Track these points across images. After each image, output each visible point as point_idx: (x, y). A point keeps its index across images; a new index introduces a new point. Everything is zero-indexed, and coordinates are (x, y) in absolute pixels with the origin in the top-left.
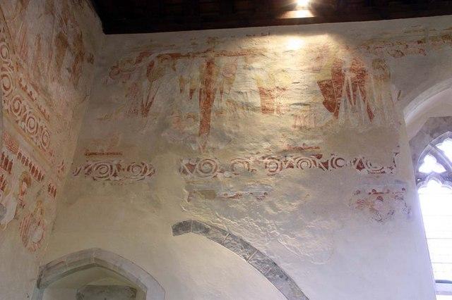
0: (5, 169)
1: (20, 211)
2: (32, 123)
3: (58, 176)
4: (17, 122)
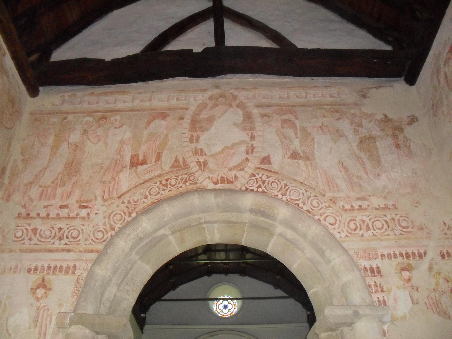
0: (375, 276)
1: (416, 295)
2: (379, 224)
4: (362, 236)
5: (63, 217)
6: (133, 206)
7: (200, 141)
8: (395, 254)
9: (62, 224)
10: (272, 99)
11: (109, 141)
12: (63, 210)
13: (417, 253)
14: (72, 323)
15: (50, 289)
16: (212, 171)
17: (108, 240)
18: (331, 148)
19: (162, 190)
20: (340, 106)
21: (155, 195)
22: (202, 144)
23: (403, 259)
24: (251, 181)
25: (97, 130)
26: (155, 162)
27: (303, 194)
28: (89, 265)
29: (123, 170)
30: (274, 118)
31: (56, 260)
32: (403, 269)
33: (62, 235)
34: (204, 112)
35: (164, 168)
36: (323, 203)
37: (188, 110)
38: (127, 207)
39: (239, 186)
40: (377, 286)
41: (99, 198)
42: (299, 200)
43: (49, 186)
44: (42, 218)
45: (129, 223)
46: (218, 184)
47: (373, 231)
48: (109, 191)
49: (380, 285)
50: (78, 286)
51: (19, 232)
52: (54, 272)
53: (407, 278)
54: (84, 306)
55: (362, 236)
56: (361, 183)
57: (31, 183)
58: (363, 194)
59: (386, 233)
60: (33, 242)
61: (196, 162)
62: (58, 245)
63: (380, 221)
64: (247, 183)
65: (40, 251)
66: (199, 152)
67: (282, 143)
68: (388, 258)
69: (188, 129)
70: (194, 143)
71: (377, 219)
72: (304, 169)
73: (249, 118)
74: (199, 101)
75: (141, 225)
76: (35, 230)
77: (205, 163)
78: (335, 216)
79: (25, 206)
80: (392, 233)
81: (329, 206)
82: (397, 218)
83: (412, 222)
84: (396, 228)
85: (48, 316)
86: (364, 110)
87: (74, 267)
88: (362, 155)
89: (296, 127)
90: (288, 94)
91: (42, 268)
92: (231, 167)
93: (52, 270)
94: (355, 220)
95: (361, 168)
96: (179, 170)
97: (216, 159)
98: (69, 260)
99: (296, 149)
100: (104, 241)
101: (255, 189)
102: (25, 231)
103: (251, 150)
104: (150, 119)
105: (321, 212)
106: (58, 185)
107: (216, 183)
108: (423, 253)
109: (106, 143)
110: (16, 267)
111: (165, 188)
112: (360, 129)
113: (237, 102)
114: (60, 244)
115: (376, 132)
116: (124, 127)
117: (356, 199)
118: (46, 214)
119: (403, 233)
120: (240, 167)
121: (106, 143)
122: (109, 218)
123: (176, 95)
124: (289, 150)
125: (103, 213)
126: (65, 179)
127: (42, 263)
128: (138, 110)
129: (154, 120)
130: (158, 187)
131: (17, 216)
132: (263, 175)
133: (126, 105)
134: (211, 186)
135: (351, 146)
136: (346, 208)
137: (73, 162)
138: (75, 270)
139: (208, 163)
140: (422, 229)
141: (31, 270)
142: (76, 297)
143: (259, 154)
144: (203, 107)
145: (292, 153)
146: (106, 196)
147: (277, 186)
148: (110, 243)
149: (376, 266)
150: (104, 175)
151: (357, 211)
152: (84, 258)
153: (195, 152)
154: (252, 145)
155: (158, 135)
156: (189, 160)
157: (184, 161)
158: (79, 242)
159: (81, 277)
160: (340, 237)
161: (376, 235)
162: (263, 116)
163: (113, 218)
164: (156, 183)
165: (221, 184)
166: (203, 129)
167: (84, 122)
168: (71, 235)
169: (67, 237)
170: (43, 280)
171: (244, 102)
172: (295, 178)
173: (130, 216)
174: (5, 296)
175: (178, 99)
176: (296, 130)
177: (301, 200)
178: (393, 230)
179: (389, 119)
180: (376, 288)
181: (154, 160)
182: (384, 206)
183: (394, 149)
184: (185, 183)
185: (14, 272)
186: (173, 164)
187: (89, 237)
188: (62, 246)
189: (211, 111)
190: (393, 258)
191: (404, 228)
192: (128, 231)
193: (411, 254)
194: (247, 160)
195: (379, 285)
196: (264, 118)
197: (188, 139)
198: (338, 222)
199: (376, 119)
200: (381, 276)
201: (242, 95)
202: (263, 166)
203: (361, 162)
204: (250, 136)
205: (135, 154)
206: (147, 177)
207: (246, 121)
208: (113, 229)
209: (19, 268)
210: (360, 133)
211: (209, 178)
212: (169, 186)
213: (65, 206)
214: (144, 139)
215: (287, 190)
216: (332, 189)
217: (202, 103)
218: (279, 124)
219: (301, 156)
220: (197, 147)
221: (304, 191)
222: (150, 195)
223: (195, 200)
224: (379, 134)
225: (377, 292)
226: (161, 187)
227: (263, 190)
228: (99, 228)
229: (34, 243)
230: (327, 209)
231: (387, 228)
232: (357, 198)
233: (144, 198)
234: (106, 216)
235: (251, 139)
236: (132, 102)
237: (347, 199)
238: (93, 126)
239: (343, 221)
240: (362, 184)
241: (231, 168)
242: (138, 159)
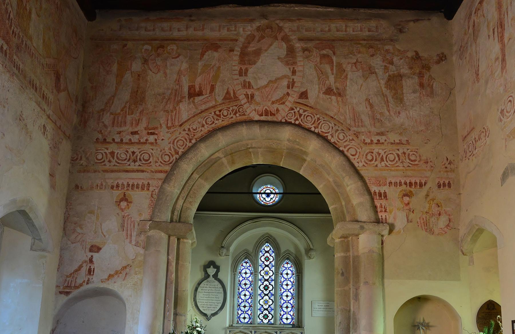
0: (381, 199)
1: (411, 216)
2: (391, 157)
3: (447, 172)
4: (377, 166)
5: (135, 142)
6: (192, 133)
8: (400, 182)
9: (135, 148)
11: (168, 71)
12: (134, 136)
13: (418, 183)
14: (151, 228)
15: (131, 202)
16: (258, 104)
17: (173, 162)
18: (362, 85)
19: (216, 120)
20: (376, 41)
21: (211, 124)
22: (249, 78)
23: (407, 187)
24: (290, 114)
25: (156, 59)
26: (210, 93)
27: (332, 128)
28: (160, 183)
29: (183, 100)
31: (133, 179)
32: (405, 195)
33: (135, 158)
34: (251, 45)
35: (217, 100)
36: (348, 136)
37: (238, 42)
38: (188, 134)
39: (280, 119)
40: (382, 207)
41: (164, 126)
42: (329, 132)
43: (119, 114)
44: (117, 143)
45: (190, 149)
46: (263, 116)
47: (386, 162)
48: (172, 120)
49: (385, 207)
50: (153, 199)
51: (100, 155)
52: (132, 189)
53: (406, 202)
54: (159, 215)
55: (377, 166)
56: (382, 120)
57: (103, 110)
58: (383, 130)
59: (397, 165)
60: (112, 164)
61: (245, 94)
62: (133, 166)
63: (393, 154)
64: (287, 116)
65: (119, 171)
66: (247, 85)
67: (319, 79)
68: (395, 186)
71: (391, 152)
72: (336, 104)
74: (247, 32)
75: (200, 151)
76: (112, 153)
77: (252, 96)
78: (357, 149)
79: (101, 131)
80: (401, 165)
81: (352, 139)
82: (407, 152)
83: (420, 156)
84: (405, 161)
85: (132, 222)
86: (397, 47)
87: (148, 185)
88: (387, 92)
89: (333, 63)
90: (329, 27)
91: (122, 185)
92: (274, 100)
93: (130, 187)
94: (373, 153)
95: (385, 105)
96: (230, 102)
97: (262, 93)
98: (143, 179)
99: (330, 85)
100: (171, 163)
101: (293, 122)
102: (104, 154)
103: (291, 85)
104: (204, 49)
105: (345, 144)
106: (127, 113)
107: (261, 115)
108: (423, 183)
109: (165, 73)
110: (102, 184)
111: (219, 118)
112: (391, 66)
113: (282, 34)
114: (135, 166)
115: (405, 70)
116: (181, 57)
117: (376, 134)
118: (120, 140)
119: (410, 165)
120: (281, 101)
121: (165, 73)
122: (173, 143)
123: (227, 24)
124: (325, 85)
125: (168, 140)
126: (133, 108)
127: (123, 181)
128: (192, 40)
129: (207, 51)
130: (213, 117)
131: (95, 140)
132: (300, 109)
133: (181, 33)
134: (257, 118)
135: (379, 83)
136: (366, 141)
137: (137, 91)
138: (149, 187)
139: (255, 96)
140: (427, 162)
141: (114, 187)
142: (152, 208)
143: (298, 89)
144: (250, 38)
145: (327, 89)
146: (170, 125)
147: (311, 119)
148: (175, 165)
149: (384, 192)
150: (166, 105)
151: (376, 145)
152: (156, 178)
153: (244, 85)
154: (293, 79)
155: (211, 66)
156: (238, 92)
157: (234, 93)
158: (150, 164)
159: (154, 193)
160: (358, 166)
161: (387, 166)
162: (304, 50)
163: (177, 144)
164: (211, 113)
165: (265, 116)
166: (251, 62)
167: (143, 50)
168: (143, 158)
169: (140, 160)
170: (125, 195)
172: (327, 112)
173: (190, 142)
174: (96, 208)
175: (228, 30)
176: (333, 67)
177: (330, 133)
178: (402, 162)
179: (419, 57)
180: (381, 209)
181: (208, 91)
182: (399, 142)
183: (417, 87)
184: (235, 114)
185: (101, 188)
186: (225, 96)
187: (158, 159)
188: (136, 168)
190: (398, 186)
191: (412, 161)
192: (190, 155)
193: (413, 183)
194: (288, 94)
195: (383, 207)
196: (305, 52)
197: (237, 72)
198: (358, 154)
199: (407, 56)
200: (387, 199)
201: (287, 26)
202: (301, 101)
203: (386, 100)
204: (291, 70)
205: (192, 85)
206: (203, 107)
208: (177, 153)
209: (104, 185)
210: (389, 71)
211: (255, 110)
212: (222, 116)
213: (136, 133)
214: (199, 71)
215: (319, 124)
216: (357, 124)
218: (318, 59)
219: (334, 92)
220: (245, 80)
221: (333, 125)
222: (207, 124)
223: (244, 131)
224: (406, 72)
225: (381, 211)
226: (215, 117)
227: (299, 123)
228: (166, 152)
229: (113, 165)
230: (351, 142)
231: (398, 160)
232: (377, 133)
233: (201, 126)
234: (171, 142)
236: (186, 31)
237: (369, 134)
238: (152, 55)
239: (362, 153)
240: (383, 121)
241: (274, 102)
242: (195, 90)
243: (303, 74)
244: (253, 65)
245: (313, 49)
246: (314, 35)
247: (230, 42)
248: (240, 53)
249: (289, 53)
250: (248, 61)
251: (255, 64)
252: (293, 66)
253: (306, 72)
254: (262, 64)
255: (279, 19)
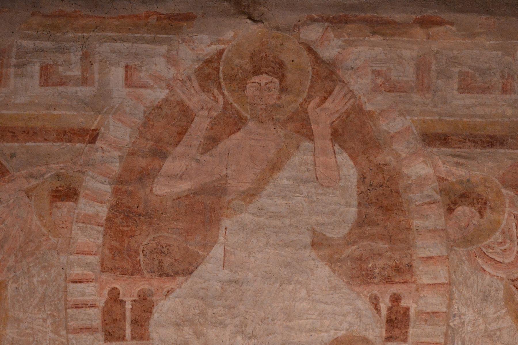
7: (150, 329)
10: (508, 96)
30: (506, 215)
69: (94, 259)
70: (123, 338)
73: (386, 209)
74: (149, 91)
123: (38, 44)
166: (168, 260)
171: (368, 107)
189: (206, 157)
196: (460, 210)
207: (373, 223)
217: (166, 100)
235: (387, 331)
243: (446, 335)
244: (180, 279)
245: (499, 194)
246: (509, 111)
247: (56, 147)
248: (114, 208)
249: (372, 211)
250: (151, 252)
251: (188, 273)
252: (395, 289)
253: (463, 323)
254: (225, 274)
255: (327, 20)
